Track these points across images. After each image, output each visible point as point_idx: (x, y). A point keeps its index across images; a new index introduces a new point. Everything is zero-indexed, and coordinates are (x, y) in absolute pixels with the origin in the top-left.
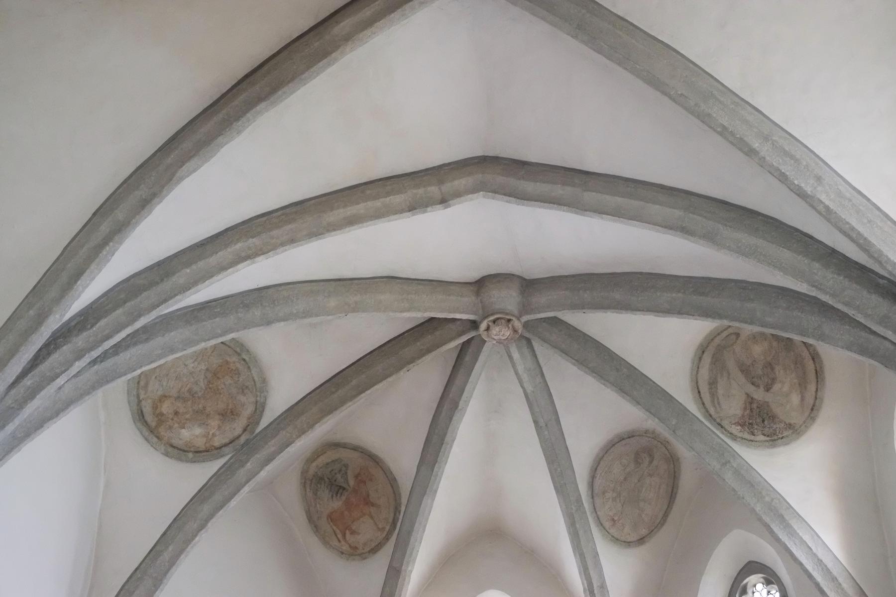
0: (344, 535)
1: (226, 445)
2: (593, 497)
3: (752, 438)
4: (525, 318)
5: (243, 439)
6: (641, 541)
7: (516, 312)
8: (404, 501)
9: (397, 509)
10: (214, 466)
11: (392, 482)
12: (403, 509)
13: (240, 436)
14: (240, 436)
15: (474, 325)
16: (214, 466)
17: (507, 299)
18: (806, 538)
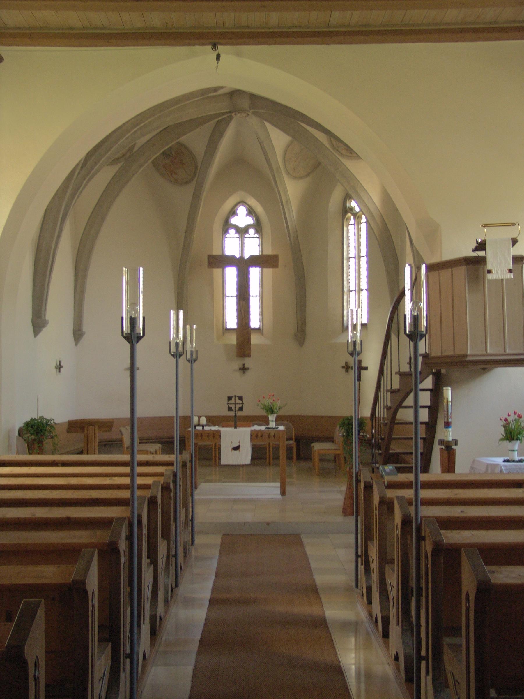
0: (171, 174)
1: (121, 157)
2: (285, 162)
3: (351, 155)
4: (251, 111)
5: (128, 155)
6: (308, 175)
7: (248, 109)
8: (199, 164)
9: (196, 168)
10: (117, 167)
11: (193, 157)
12: (199, 168)
13: (126, 154)
14: (126, 154)
15: (230, 112)
16: (117, 167)
17: (245, 103)
18: (366, 200)
